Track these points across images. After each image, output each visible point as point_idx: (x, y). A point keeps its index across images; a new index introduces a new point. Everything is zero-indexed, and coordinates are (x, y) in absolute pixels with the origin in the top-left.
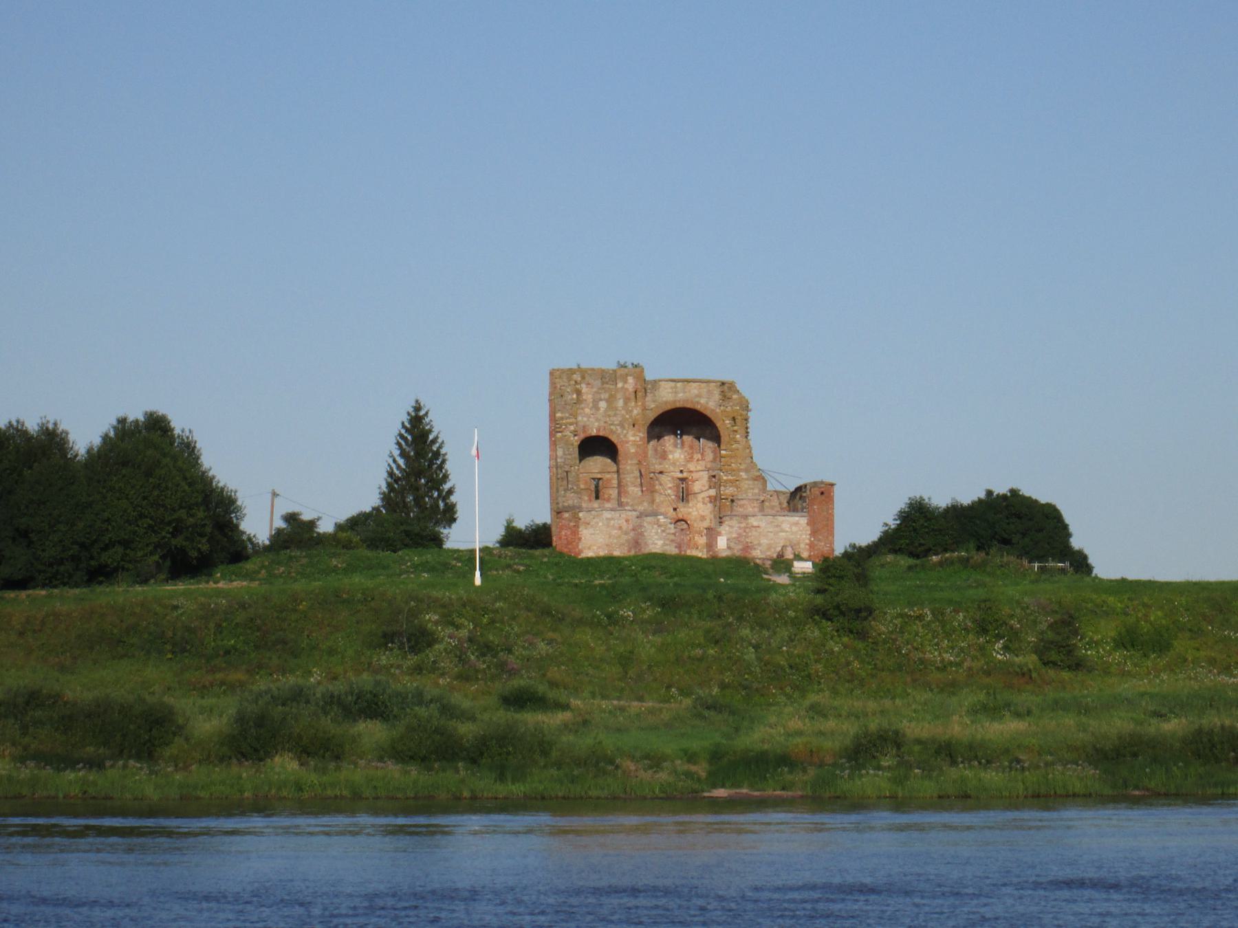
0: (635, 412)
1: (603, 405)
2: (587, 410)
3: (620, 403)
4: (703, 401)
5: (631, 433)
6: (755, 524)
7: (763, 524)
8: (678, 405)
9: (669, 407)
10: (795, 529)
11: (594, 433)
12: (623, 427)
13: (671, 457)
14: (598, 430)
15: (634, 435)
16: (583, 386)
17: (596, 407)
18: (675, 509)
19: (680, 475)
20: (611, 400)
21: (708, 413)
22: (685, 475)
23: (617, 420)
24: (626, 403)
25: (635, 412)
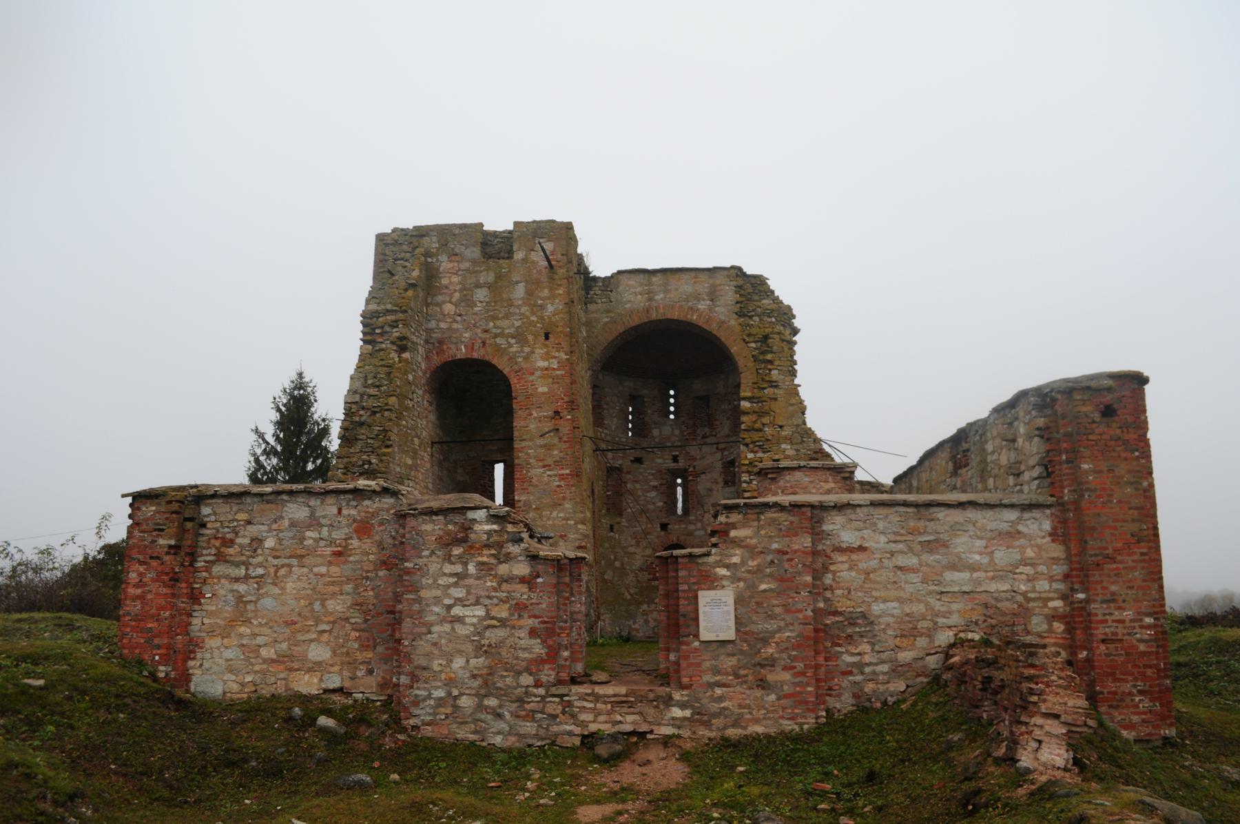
0: (550, 308)
1: (481, 294)
2: (449, 308)
3: (520, 291)
4: (703, 305)
5: (540, 351)
6: (848, 537)
7: (878, 542)
8: (654, 316)
9: (637, 321)
10: (1003, 556)
11: (462, 352)
12: (519, 336)
13: (656, 432)
14: (471, 348)
15: (547, 357)
16: (444, 258)
17: (467, 301)
18: (664, 527)
19: (672, 465)
20: (498, 287)
21: (713, 328)
22: (682, 463)
23: (510, 325)
24: (530, 293)
25: (550, 308)
